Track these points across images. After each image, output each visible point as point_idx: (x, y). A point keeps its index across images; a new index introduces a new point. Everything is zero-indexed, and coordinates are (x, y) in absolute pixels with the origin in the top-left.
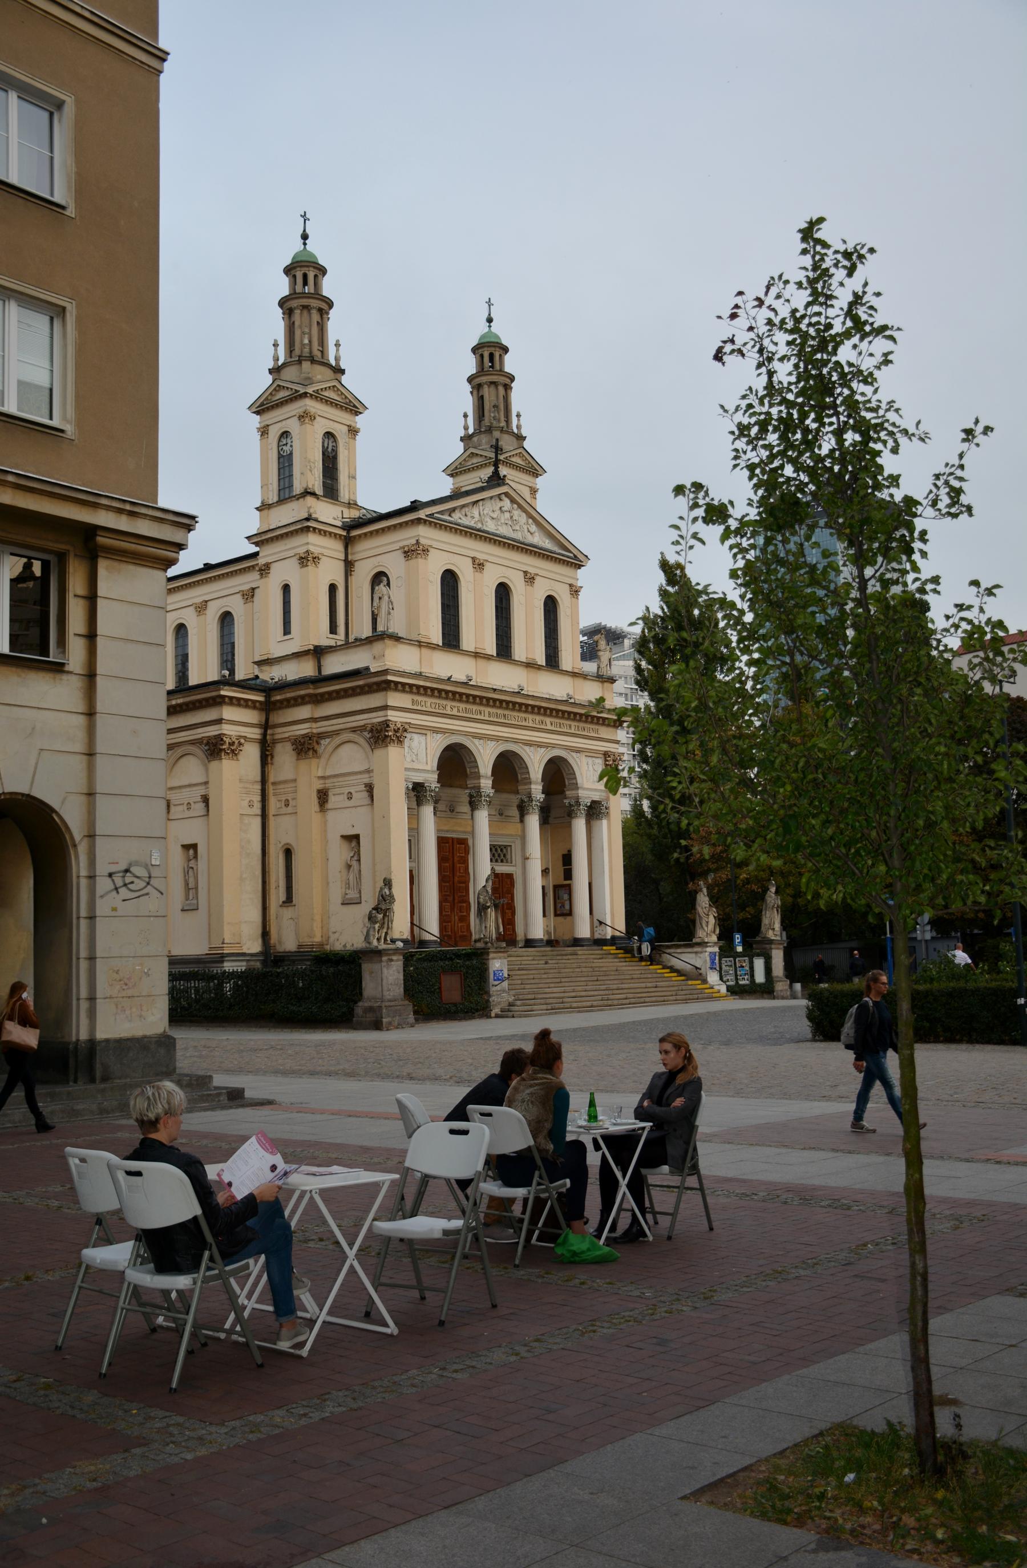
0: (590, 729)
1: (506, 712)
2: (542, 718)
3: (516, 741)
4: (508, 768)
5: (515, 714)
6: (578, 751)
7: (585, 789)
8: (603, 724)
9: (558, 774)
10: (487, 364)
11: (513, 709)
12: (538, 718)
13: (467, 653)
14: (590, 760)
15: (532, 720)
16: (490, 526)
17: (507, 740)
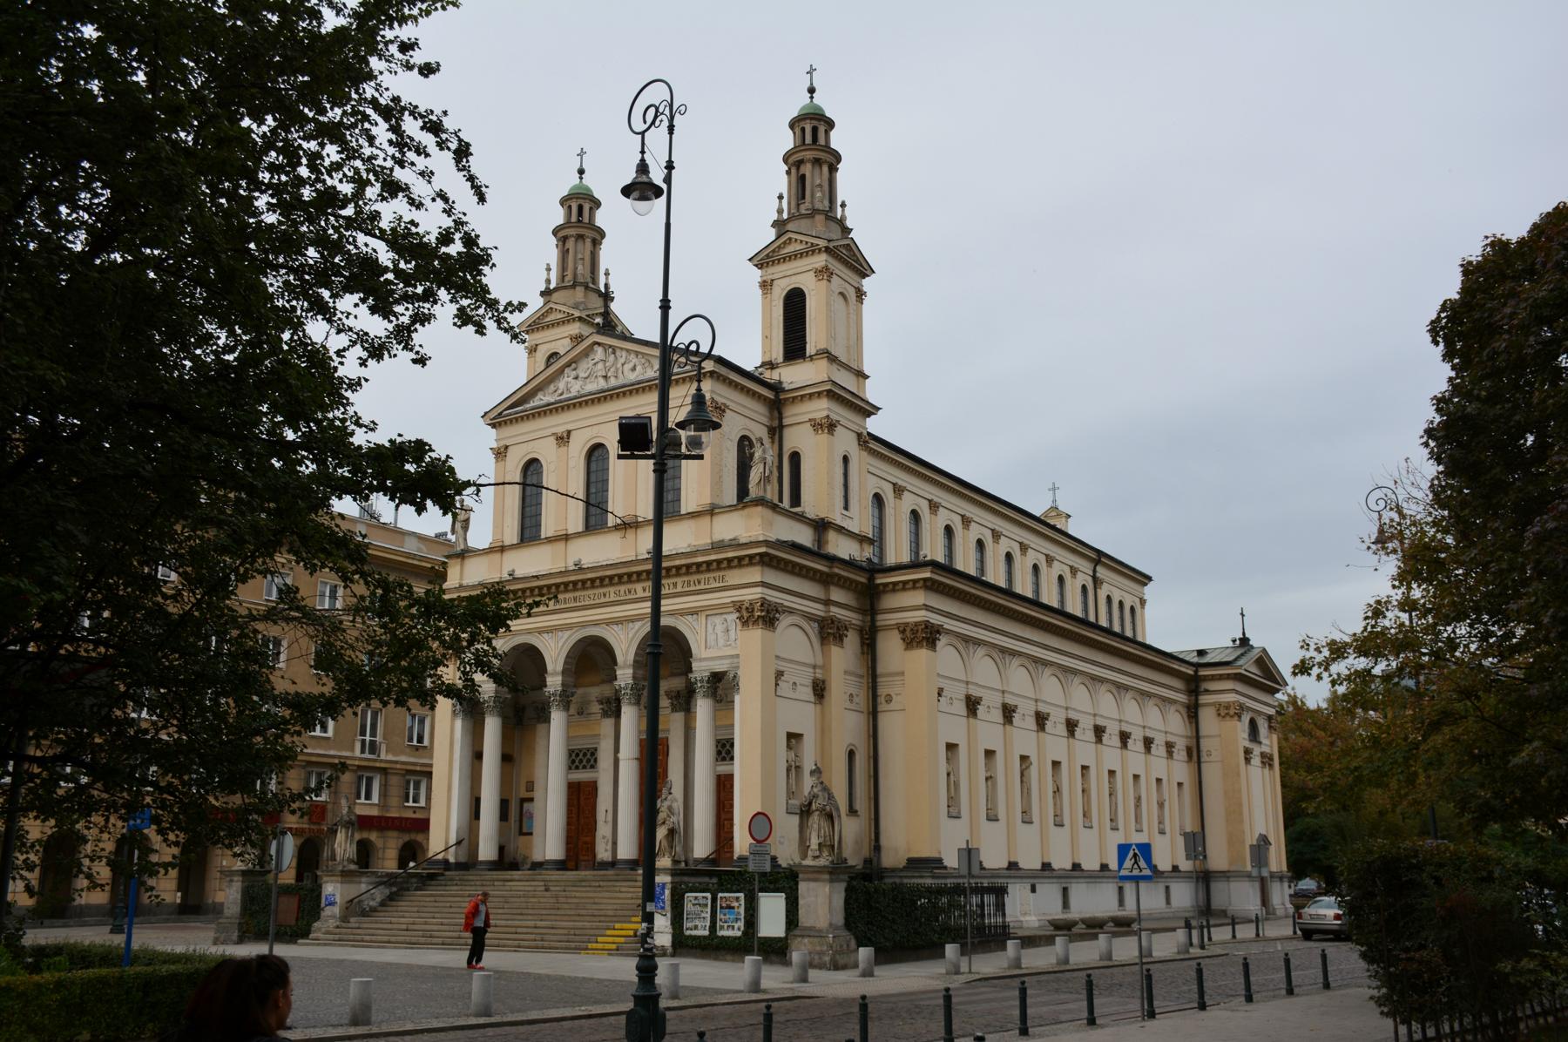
0: (710, 580)
1: (577, 594)
2: (630, 586)
3: (596, 624)
4: (591, 657)
5: (591, 592)
6: (694, 612)
7: (701, 660)
8: (730, 567)
9: (665, 650)
10: (808, 140)
11: (584, 588)
12: (623, 588)
13: (550, 540)
14: (718, 620)
15: (612, 593)
16: (591, 387)
17: (583, 625)
